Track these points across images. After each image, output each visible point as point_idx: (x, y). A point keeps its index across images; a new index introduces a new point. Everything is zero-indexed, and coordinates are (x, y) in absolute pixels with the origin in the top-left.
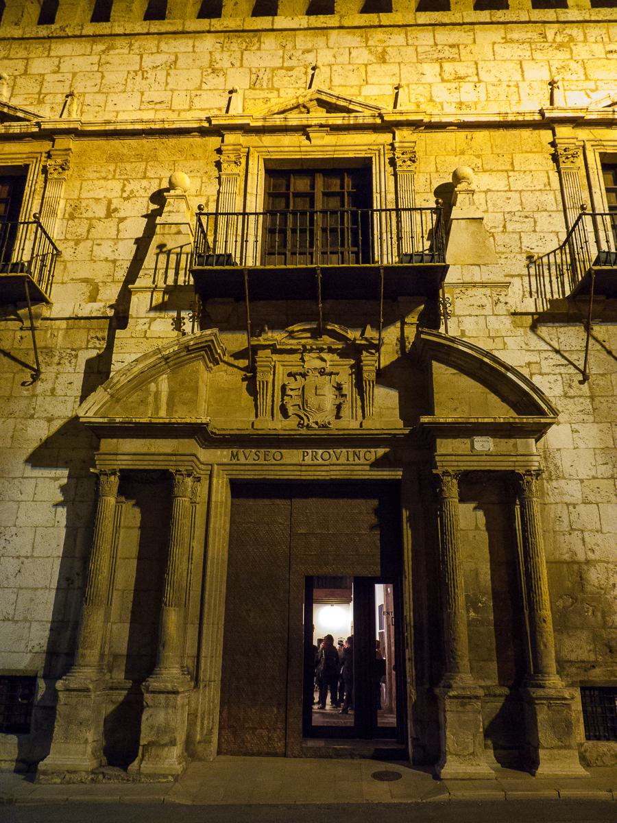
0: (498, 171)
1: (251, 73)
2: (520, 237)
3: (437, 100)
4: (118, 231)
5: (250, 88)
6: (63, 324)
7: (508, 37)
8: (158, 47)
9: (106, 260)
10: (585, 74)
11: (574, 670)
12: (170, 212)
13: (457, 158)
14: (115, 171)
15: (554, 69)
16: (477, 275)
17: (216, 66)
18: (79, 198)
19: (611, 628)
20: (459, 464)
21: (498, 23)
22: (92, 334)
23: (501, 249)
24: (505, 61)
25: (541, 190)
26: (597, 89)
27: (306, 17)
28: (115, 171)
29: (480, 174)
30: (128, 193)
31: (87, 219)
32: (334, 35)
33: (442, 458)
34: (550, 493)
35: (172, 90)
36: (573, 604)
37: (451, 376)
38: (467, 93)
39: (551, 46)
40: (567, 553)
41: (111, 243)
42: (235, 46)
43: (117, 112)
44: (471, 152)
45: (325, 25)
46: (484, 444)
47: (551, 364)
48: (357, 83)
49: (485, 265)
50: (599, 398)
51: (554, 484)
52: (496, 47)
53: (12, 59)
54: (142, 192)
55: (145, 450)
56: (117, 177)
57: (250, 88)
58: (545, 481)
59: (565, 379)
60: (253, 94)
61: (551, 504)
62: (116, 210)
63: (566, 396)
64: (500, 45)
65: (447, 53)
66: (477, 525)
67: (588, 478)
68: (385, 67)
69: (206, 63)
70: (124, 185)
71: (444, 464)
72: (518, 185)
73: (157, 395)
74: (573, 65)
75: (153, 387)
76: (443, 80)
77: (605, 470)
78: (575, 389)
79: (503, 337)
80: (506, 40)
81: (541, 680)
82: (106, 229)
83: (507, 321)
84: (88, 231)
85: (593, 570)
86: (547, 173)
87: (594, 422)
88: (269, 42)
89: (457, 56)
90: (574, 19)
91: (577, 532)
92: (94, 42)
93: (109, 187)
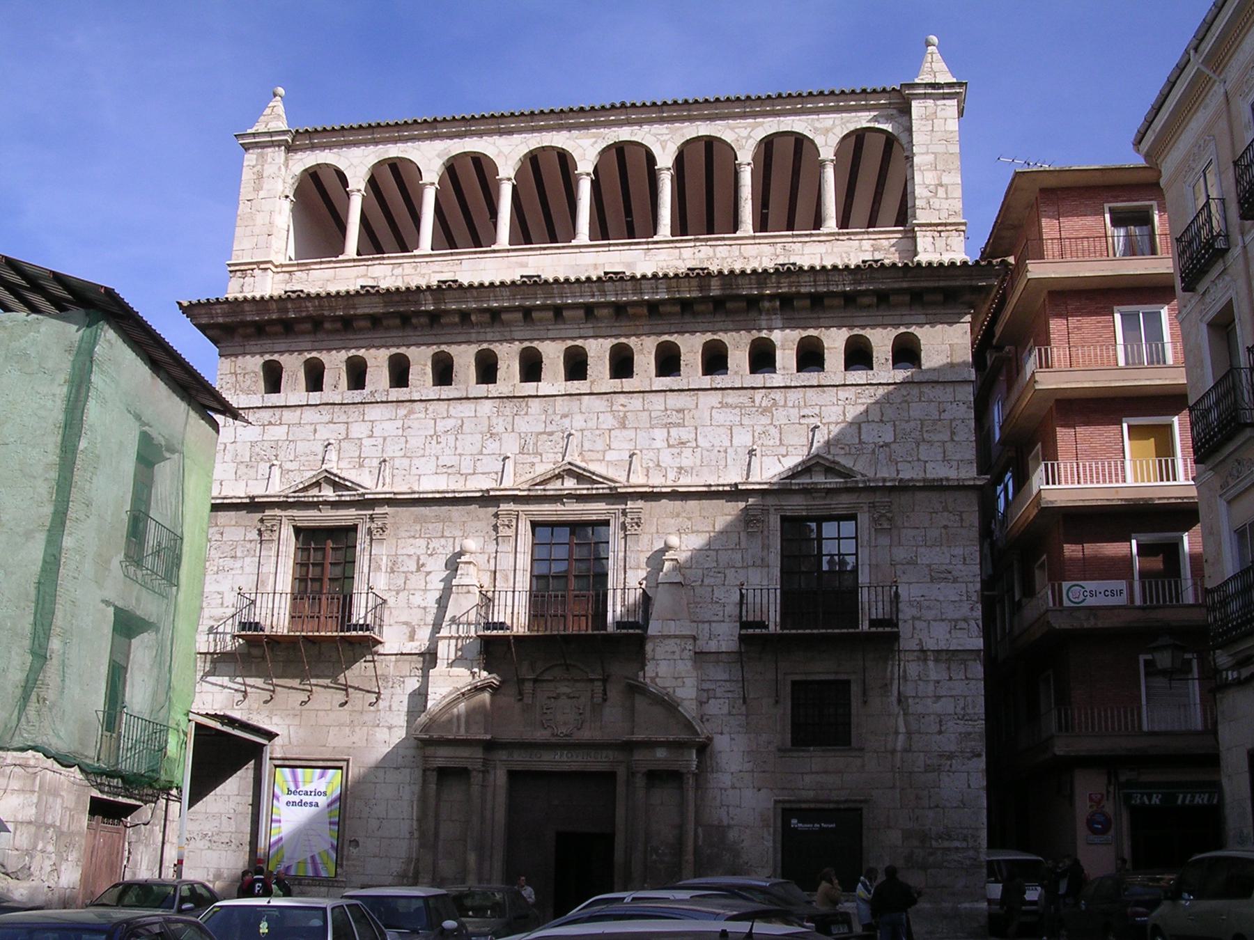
0: (703, 532)
2: (713, 590)
4: (426, 583)
5: (520, 453)
8: (448, 411)
10: (780, 439)
12: (462, 574)
14: (421, 530)
15: (756, 434)
16: (672, 628)
18: (396, 555)
21: (716, 389)
22: (413, 665)
23: (699, 600)
24: (718, 426)
25: (732, 549)
26: (787, 455)
28: (421, 530)
30: (431, 550)
31: (403, 572)
35: (460, 455)
38: (687, 459)
39: (757, 411)
42: (508, 411)
43: (420, 476)
44: (684, 515)
45: (578, 392)
46: (661, 753)
49: (679, 620)
51: (715, 775)
53: (335, 423)
55: (452, 754)
56: (422, 536)
60: (520, 458)
62: (423, 565)
63: (730, 714)
65: (675, 418)
68: (625, 432)
69: (485, 429)
70: (428, 543)
74: (773, 431)
76: (669, 446)
77: (747, 766)
80: (724, 405)
82: (416, 581)
83: (689, 664)
84: (405, 583)
86: (739, 534)
89: (681, 421)
92: (398, 406)
93: (417, 545)
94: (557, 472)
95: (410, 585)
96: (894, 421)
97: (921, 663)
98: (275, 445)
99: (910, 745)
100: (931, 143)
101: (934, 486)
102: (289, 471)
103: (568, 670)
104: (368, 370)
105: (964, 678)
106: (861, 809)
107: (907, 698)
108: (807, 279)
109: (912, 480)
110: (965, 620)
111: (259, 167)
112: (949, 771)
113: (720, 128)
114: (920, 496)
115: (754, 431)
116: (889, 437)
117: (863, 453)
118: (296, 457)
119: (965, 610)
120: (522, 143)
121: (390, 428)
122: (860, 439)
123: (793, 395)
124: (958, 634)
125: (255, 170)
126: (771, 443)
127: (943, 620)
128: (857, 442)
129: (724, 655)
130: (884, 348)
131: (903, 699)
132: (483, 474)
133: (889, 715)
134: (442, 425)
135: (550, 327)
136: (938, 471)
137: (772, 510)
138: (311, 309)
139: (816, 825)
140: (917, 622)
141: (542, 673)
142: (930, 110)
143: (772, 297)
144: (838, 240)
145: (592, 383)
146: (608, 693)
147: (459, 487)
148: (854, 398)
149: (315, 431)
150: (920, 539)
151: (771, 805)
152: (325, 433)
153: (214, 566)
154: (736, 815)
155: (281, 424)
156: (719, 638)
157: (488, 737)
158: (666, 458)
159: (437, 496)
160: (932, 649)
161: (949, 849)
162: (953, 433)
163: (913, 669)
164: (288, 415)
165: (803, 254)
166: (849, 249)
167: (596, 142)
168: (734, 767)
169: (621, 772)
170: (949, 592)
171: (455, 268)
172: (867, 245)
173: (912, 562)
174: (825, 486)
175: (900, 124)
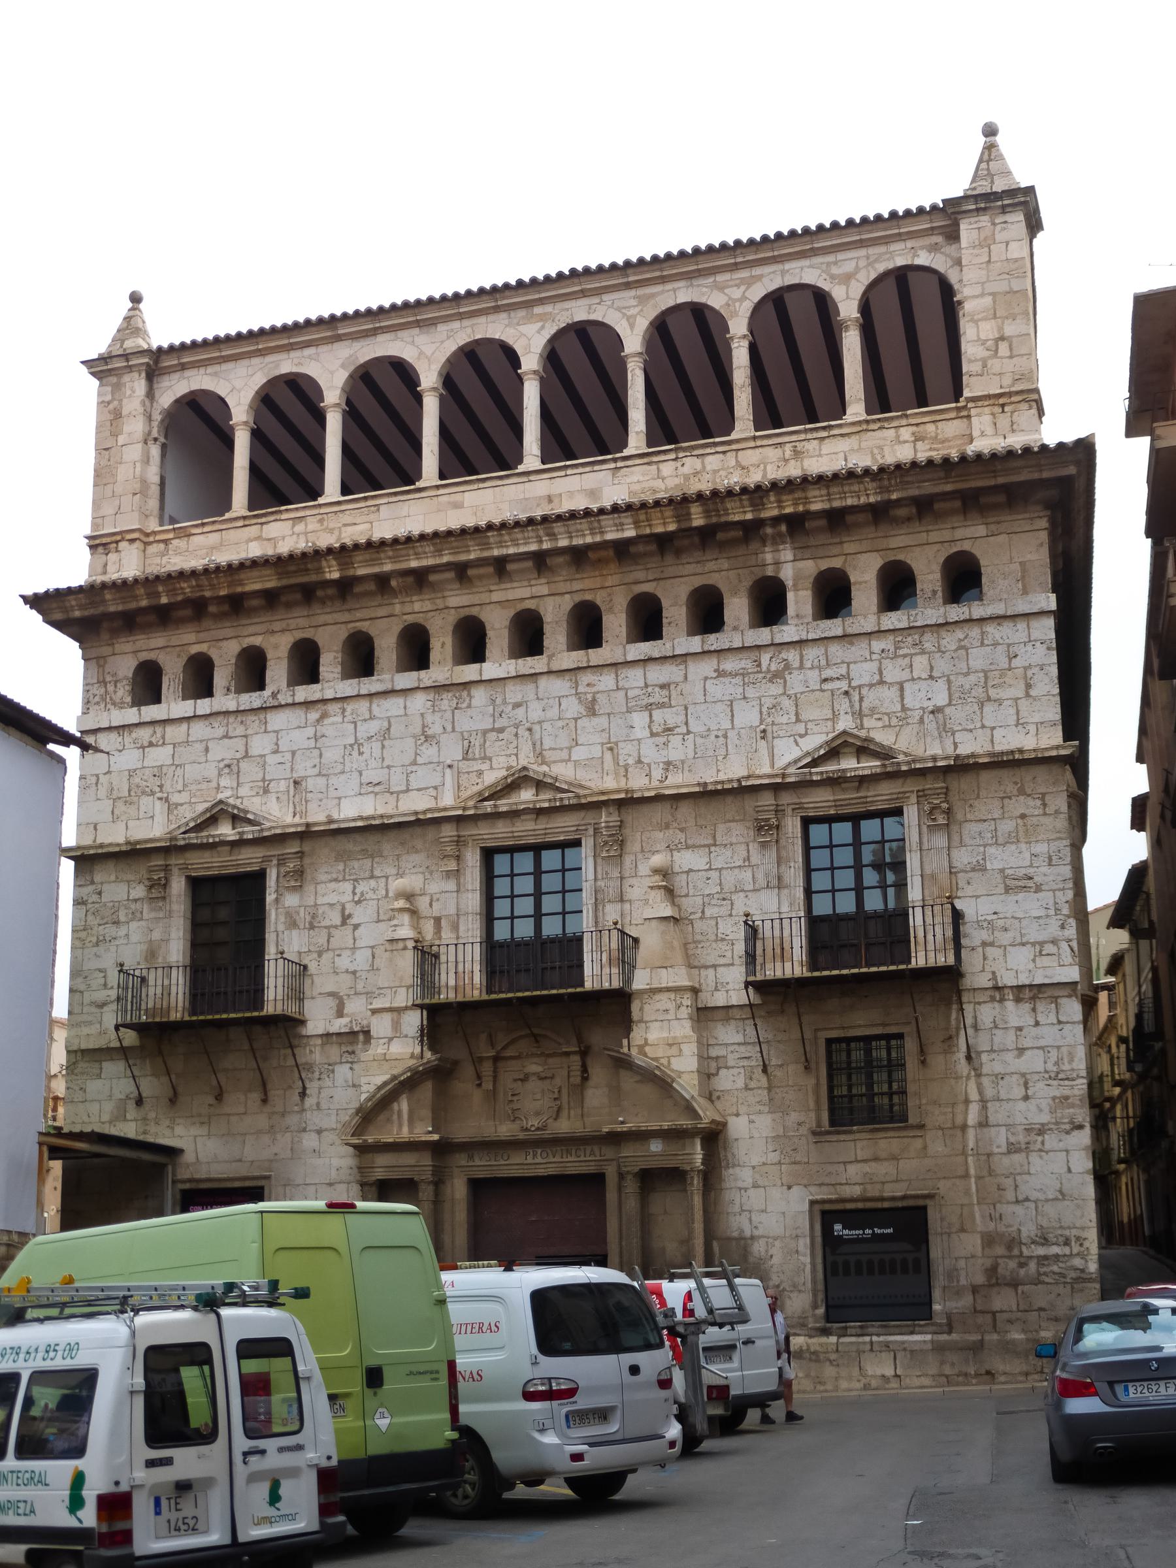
1: (464, 739)
3: (646, 760)
4: (355, 940)
5: (464, 759)
6: (319, 1041)
7: (721, 668)
8: (370, 711)
9: (347, 971)
10: (797, 714)
13: (661, 835)
15: (764, 709)
16: (667, 978)
17: (429, 732)
18: (316, 905)
23: (698, 937)
25: (740, 867)
26: (806, 734)
27: (513, 661)
29: (683, 852)
31: (326, 927)
32: (543, 682)
35: (388, 767)
38: (677, 750)
41: (348, 952)
43: (340, 798)
44: (675, 825)
45: (533, 671)
46: (656, 1146)
48: (566, 744)
51: (731, 1171)
52: (709, 682)
53: (231, 738)
54: (371, 895)
57: (464, 759)
60: (464, 765)
62: (350, 916)
63: (747, 1088)
64: (712, 681)
65: (658, 696)
68: (595, 721)
69: (418, 730)
70: (355, 888)
72: (717, 864)
73: (400, 1112)
74: (787, 703)
75: (395, 1106)
76: (653, 735)
77: (773, 1157)
80: (721, 674)
82: (342, 937)
83: (687, 1024)
84: (328, 941)
85: (756, 1244)
88: (479, 696)
89: (666, 700)
90: (789, 640)
92: (307, 709)
94: (509, 781)
95: (334, 943)
96: (948, 676)
97: (996, 1005)
98: (159, 773)
99: (987, 1117)
100: (988, 281)
101: (1003, 761)
102: (177, 805)
103: (537, 1042)
104: (268, 664)
105: (1055, 1021)
106: (924, 1209)
107: (979, 1053)
108: (817, 493)
109: (973, 755)
110: (1054, 942)
111: (116, 403)
112: (1040, 1150)
113: (705, 289)
114: (985, 776)
115: (761, 705)
116: (941, 699)
117: (908, 724)
118: (185, 785)
119: (1053, 929)
120: (448, 338)
121: (300, 738)
122: (903, 705)
123: (812, 654)
124: (1046, 961)
125: (111, 407)
126: (784, 719)
127: (1023, 944)
128: (899, 707)
129: (735, 1010)
130: (931, 577)
131: (973, 1055)
132: (419, 790)
133: (956, 1078)
134: (365, 729)
135: (493, 588)
136: (1010, 740)
137: (789, 811)
138: (188, 590)
139: (867, 1231)
140: (989, 950)
141: (504, 1048)
142: (987, 232)
143: (776, 520)
144: (867, 430)
145: (550, 657)
146: (590, 1070)
147: (389, 810)
148: (892, 649)
149: (207, 750)
150: (989, 835)
151: (806, 1206)
152: (222, 751)
153: (93, 935)
155: (164, 743)
156: (730, 986)
157: (436, 1137)
158: (650, 752)
159: (360, 824)
160: (1009, 984)
161: (1046, 1257)
162: (1028, 686)
163: (987, 1013)
164: (172, 732)
165: (820, 455)
166: (881, 443)
167: (543, 327)
168: (755, 1160)
169: (611, 1173)
170: (1030, 905)
171: (372, 517)
172: (906, 433)
173: (980, 868)
174: (857, 773)
175: (947, 255)
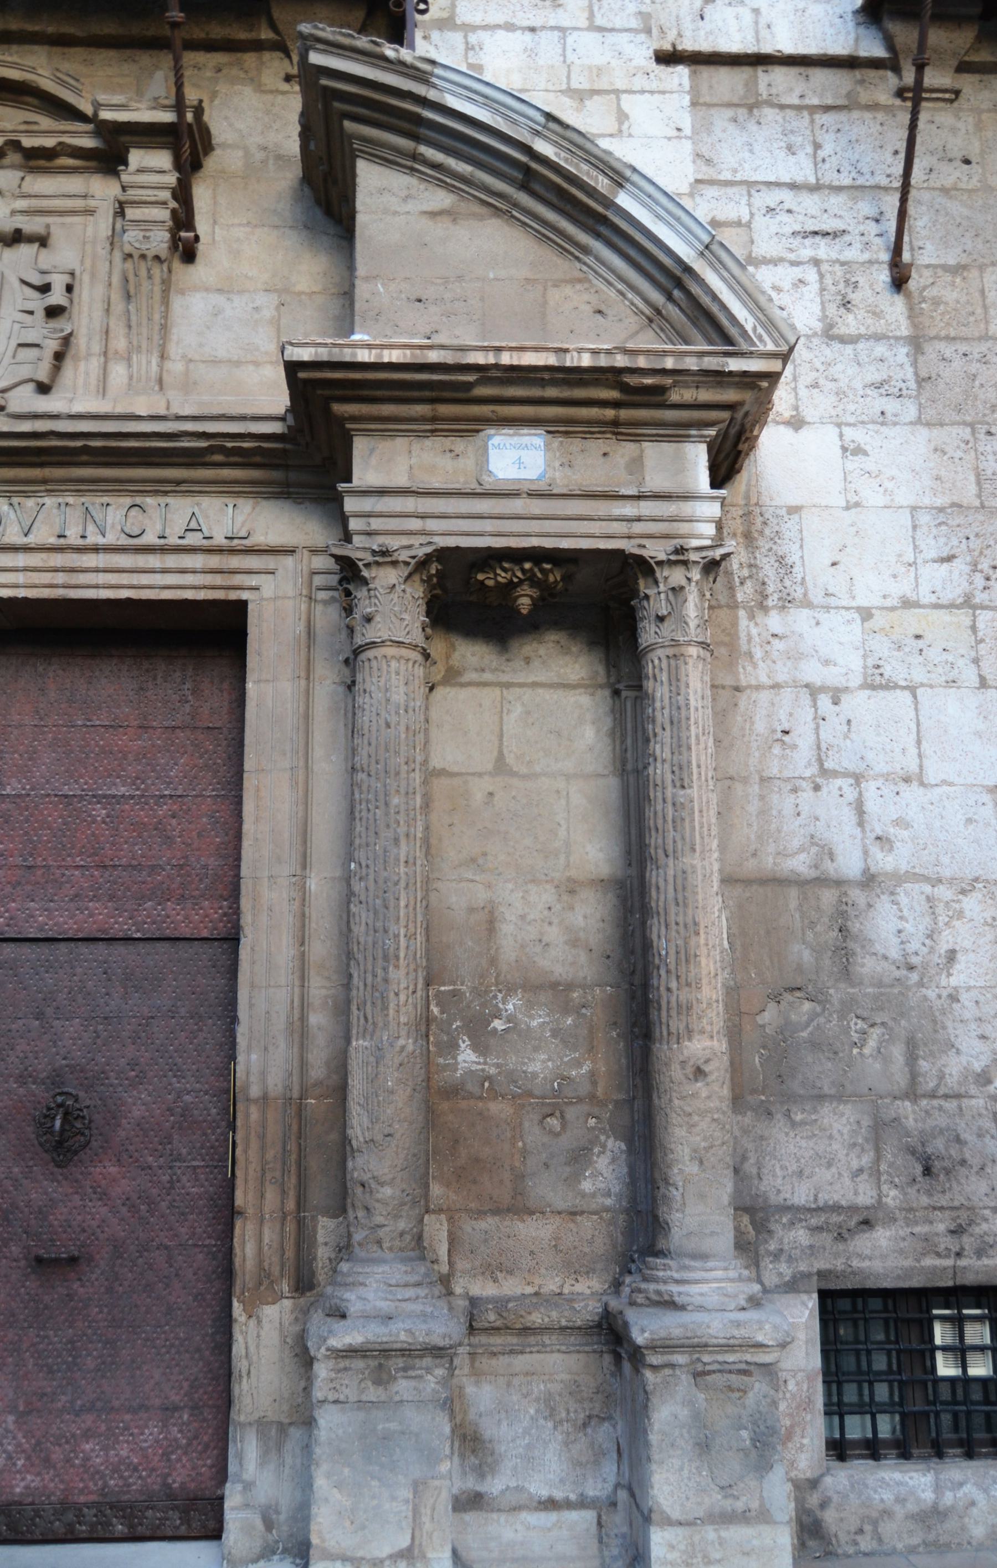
11: (801, 1236)
19: (933, 1095)
20: (432, 525)
33: (367, 504)
34: (758, 653)
36: (813, 1016)
37: (425, 222)
40: (802, 849)
47: (788, 230)
50: (941, 346)
51: (774, 622)
58: (742, 613)
59: (828, 281)
61: (758, 687)
63: (829, 334)
66: (501, 757)
67: (888, 603)
71: (376, 524)
78: (861, 314)
79: (617, 92)
81: (677, 1282)
85: (884, 906)
87: (918, 421)
91: (839, 782)
154: (900, 822)
